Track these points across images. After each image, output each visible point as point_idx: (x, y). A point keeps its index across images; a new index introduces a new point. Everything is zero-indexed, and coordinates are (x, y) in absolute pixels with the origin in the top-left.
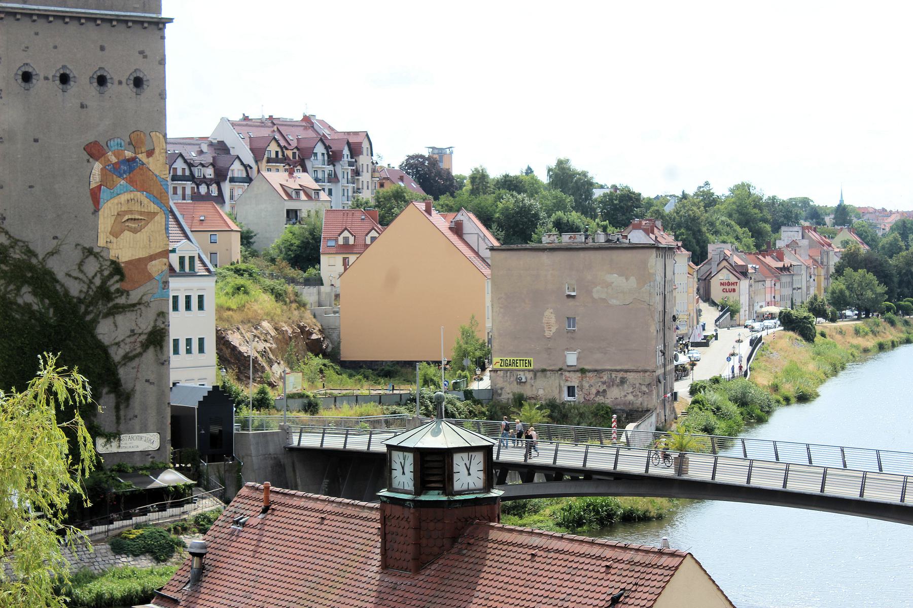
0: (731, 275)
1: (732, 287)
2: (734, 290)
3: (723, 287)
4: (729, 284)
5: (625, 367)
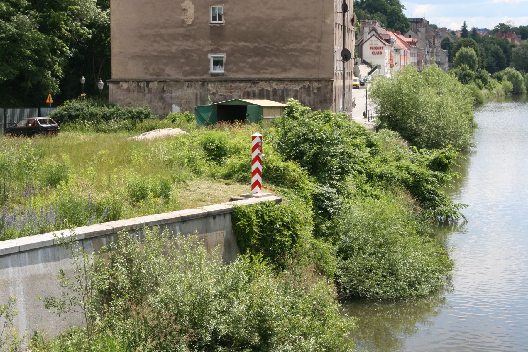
0: (379, 42)
1: (379, 51)
2: (381, 53)
3: (372, 50)
4: (377, 48)
5: (291, 75)
